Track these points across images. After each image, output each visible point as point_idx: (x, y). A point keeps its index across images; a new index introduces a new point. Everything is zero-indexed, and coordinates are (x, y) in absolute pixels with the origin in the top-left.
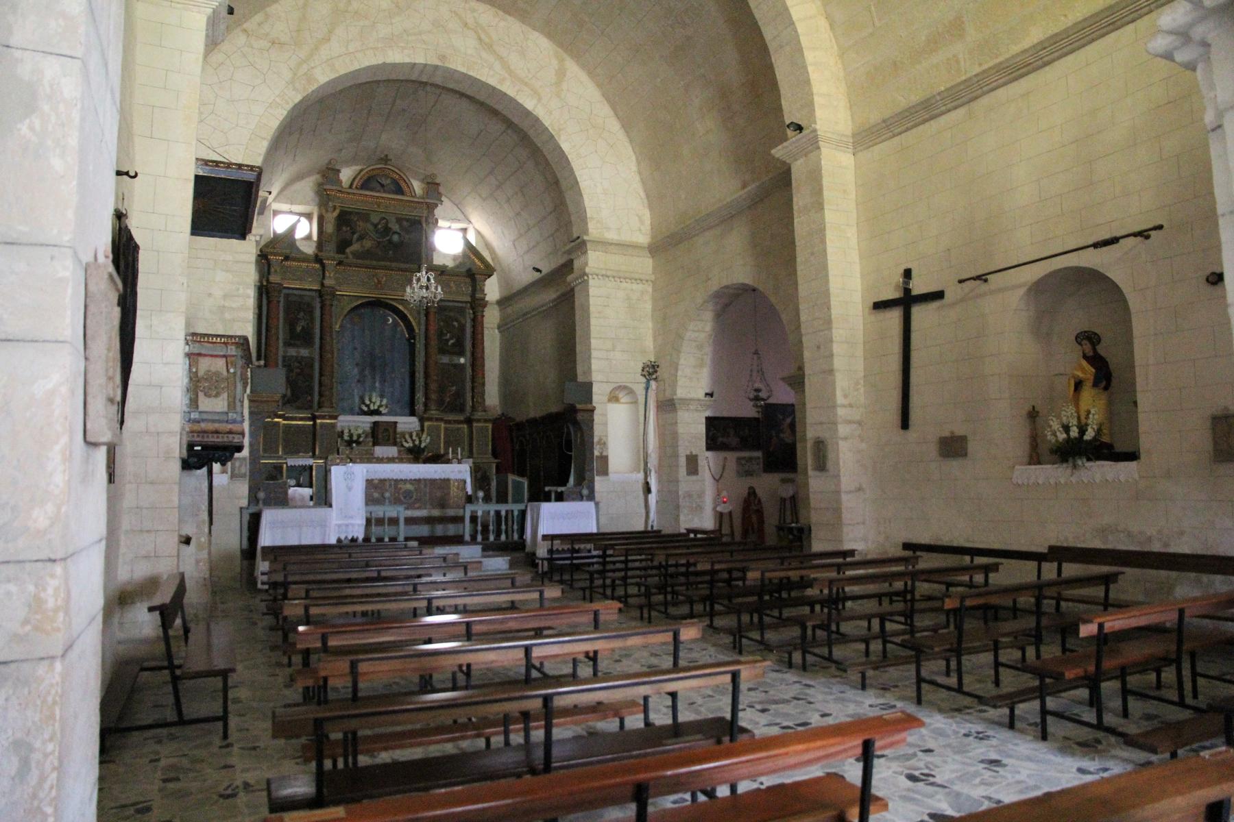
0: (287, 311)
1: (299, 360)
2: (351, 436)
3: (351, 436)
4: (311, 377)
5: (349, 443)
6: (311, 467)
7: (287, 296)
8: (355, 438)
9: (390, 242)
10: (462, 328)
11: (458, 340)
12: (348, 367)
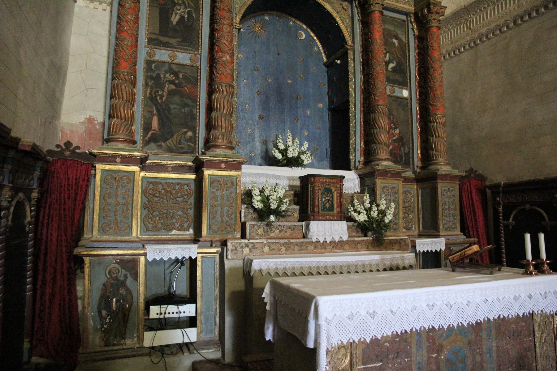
1: (174, 69)
2: (266, 200)
3: (266, 200)
4: (195, 100)
5: (263, 214)
6: (193, 262)
8: (273, 206)
10: (404, 48)
11: (398, 65)
12: (244, 93)
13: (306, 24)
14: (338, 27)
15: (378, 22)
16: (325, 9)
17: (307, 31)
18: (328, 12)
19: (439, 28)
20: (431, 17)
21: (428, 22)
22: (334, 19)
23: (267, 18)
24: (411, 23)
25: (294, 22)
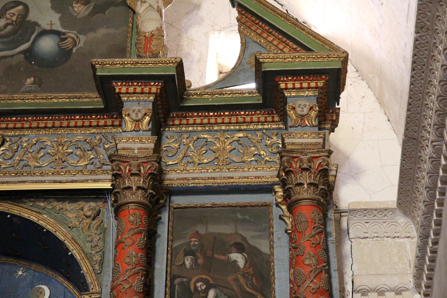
9: (30, 54)
22: (62, 243)
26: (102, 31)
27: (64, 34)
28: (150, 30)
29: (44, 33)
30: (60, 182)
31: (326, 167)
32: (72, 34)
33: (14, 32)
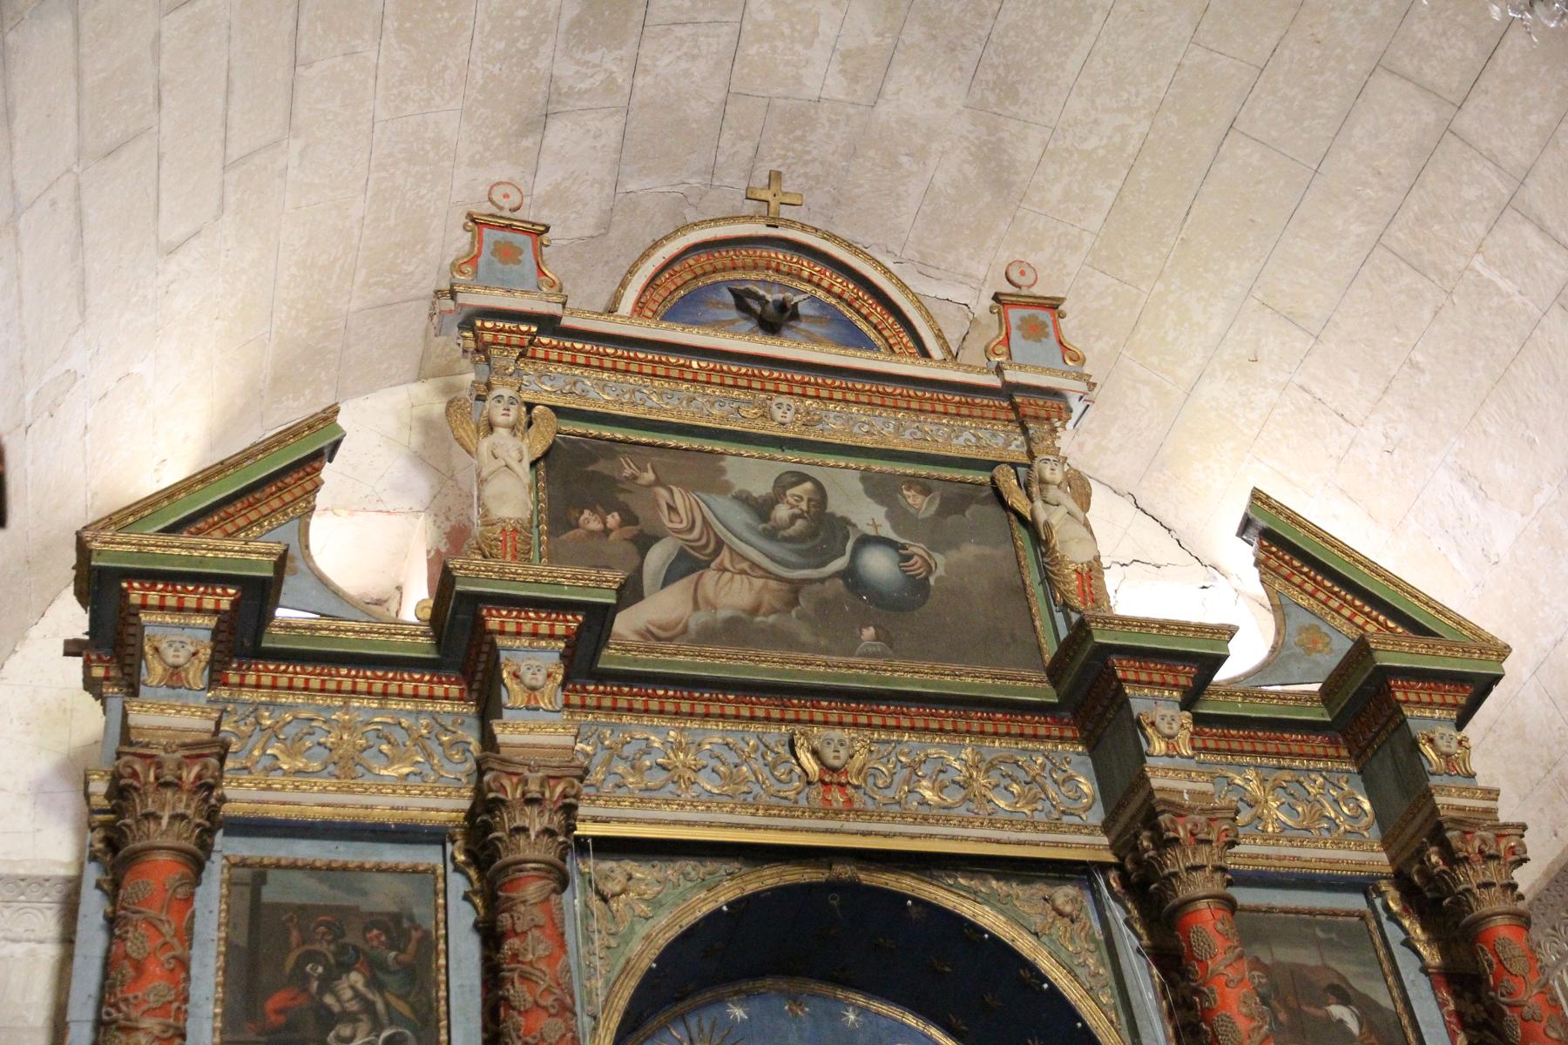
0: (247, 969)
7: (254, 876)
9: (851, 576)
13: (917, 1011)
14: (1055, 992)
15: (1218, 943)
16: (981, 930)
17: (929, 1038)
18: (995, 940)
19: (1523, 921)
20: (1469, 878)
21: (1462, 902)
22: (1031, 967)
23: (738, 1013)
24: (1393, 917)
25: (862, 1011)
26: (970, 551)
27: (904, 547)
28: (1086, 560)
29: (866, 541)
30: (783, 830)
31: (573, 801)
32: (918, 549)
33: (811, 534)
